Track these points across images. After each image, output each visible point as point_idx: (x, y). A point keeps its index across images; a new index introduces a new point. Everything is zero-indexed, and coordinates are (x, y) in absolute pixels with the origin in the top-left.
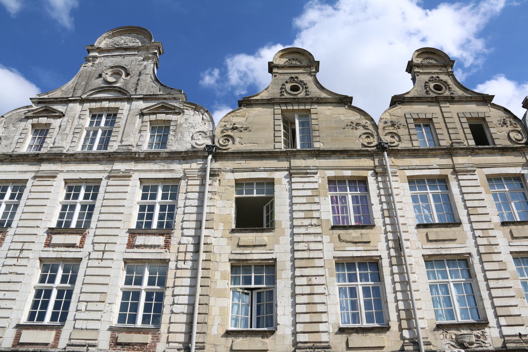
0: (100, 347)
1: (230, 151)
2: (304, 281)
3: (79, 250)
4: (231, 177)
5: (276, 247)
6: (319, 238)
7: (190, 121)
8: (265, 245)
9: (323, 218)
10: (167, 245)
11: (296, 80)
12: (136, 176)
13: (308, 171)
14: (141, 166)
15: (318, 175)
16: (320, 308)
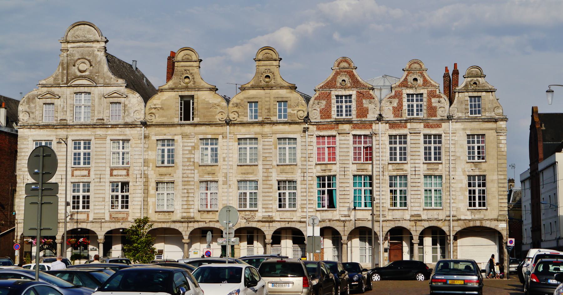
0: (106, 220)
1: (153, 123)
2: (185, 191)
3: (88, 178)
4: (154, 138)
5: (175, 175)
6: (193, 172)
7: (131, 103)
8: (170, 174)
9: (196, 161)
10: (128, 175)
11: (188, 72)
12: (109, 138)
13: (190, 136)
14: (110, 131)
15: (195, 138)
16: (191, 203)
